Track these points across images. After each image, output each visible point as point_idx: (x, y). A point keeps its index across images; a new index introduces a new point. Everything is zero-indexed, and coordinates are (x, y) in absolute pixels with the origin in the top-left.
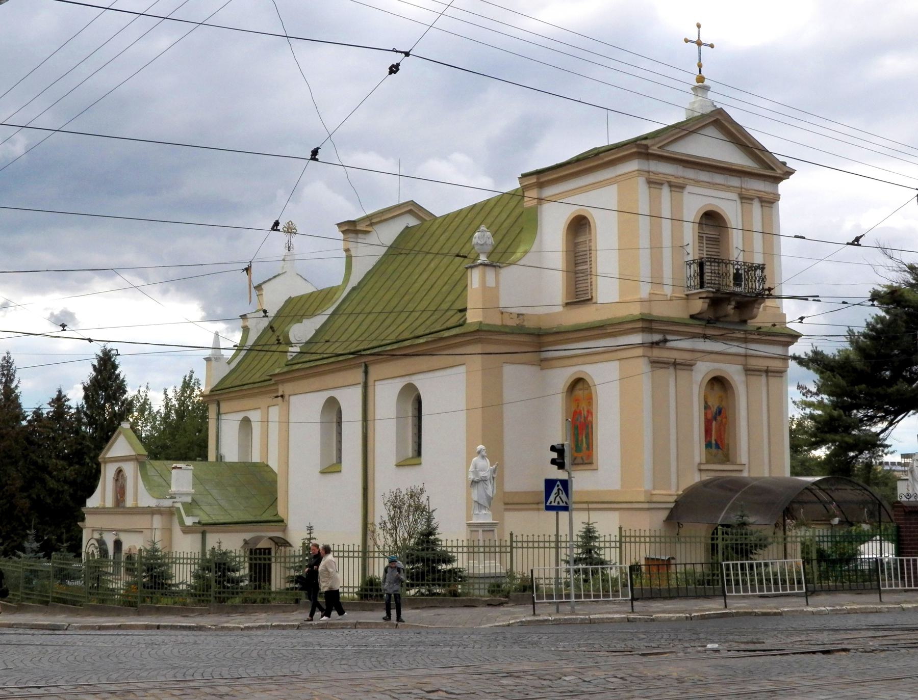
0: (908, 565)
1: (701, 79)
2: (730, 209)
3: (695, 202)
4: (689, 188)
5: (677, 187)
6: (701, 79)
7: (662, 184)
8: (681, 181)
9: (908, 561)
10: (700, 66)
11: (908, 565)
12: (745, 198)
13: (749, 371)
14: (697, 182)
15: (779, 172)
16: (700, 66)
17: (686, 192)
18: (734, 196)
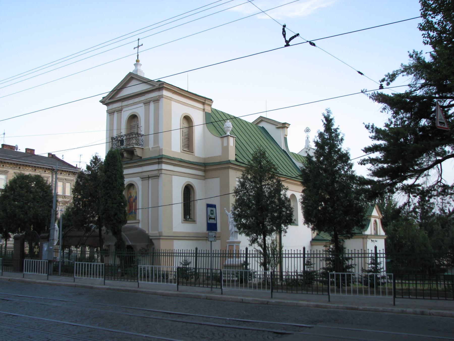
0: (42, 263)
1: (138, 61)
2: (140, 110)
3: (126, 115)
4: (124, 110)
5: (120, 111)
6: (138, 61)
7: (114, 113)
8: (120, 108)
9: (32, 261)
10: (138, 56)
11: (42, 263)
12: (147, 103)
13: (143, 179)
14: (127, 106)
15: (157, 86)
16: (138, 56)
17: (122, 112)
18: (142, 104)
